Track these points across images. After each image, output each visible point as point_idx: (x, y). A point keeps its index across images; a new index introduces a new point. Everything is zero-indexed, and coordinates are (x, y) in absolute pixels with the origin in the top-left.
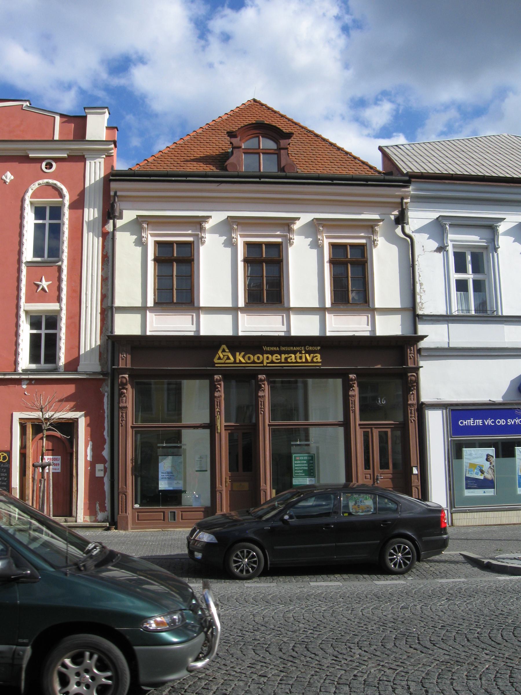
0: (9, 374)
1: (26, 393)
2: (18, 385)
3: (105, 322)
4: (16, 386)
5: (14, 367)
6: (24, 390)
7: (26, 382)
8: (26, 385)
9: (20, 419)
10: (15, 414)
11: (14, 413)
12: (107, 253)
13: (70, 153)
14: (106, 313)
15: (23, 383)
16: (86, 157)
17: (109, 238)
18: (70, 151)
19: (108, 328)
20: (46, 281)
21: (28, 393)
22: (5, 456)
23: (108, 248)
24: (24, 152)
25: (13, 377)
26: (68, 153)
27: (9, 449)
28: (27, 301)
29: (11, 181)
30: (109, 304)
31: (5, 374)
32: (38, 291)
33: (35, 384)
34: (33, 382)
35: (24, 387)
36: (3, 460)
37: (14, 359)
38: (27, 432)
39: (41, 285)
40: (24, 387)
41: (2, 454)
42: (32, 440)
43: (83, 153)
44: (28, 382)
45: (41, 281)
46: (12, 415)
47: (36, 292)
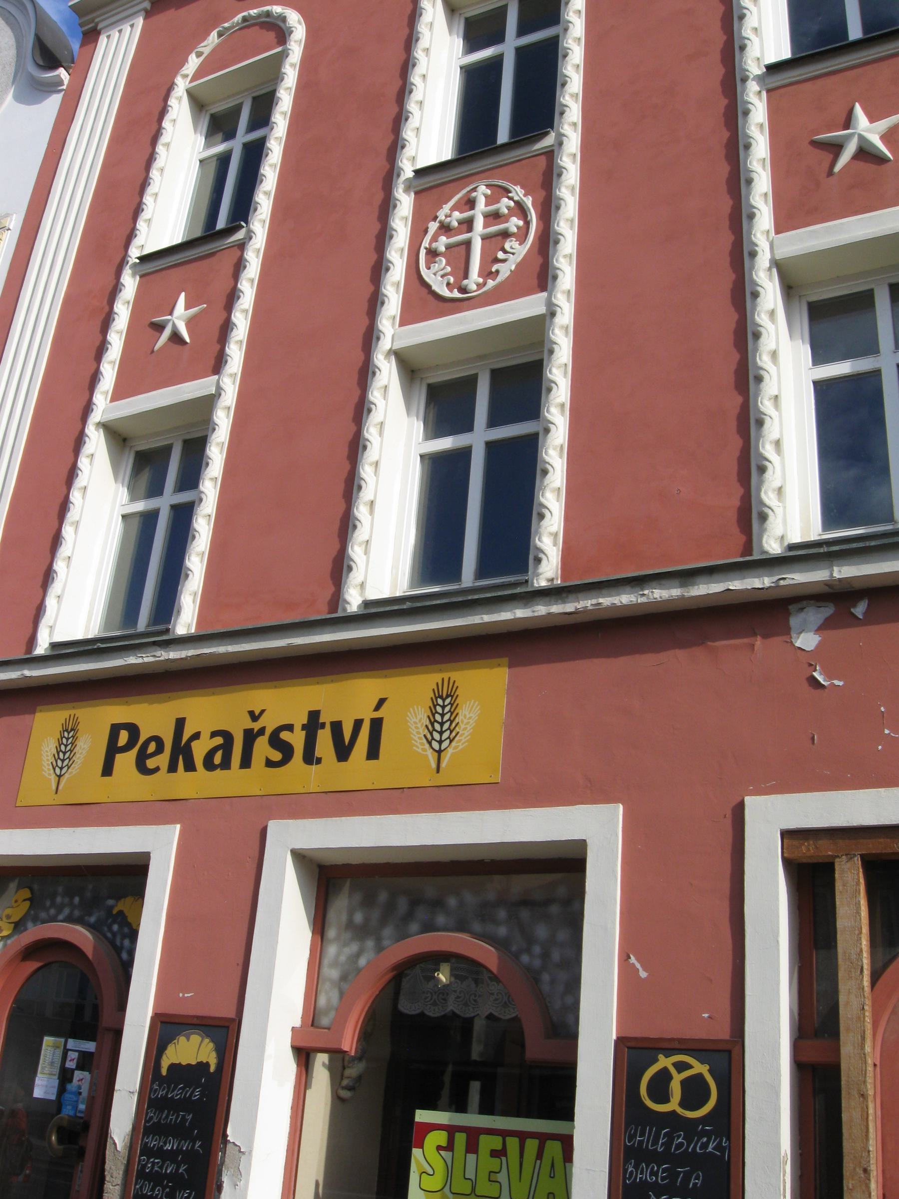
0: (710, 572)
1: (820, 678)
2: (765, 636)
4: (759, 642)
5: (743, 538)
6: (810, 659)
7: (815, 615)
8: (819, 629)
9: (786, 834)
10: (754, 805)
11: (750, 801)
15: (794, 621)
20: (873, 118)
21: (829, 676)
22: (699, 1077)
25: (738, 584)
27: (723, 1033)
31: (687, 576)
32: (837, 168)
33: (870, 619)
34: (860, 610)
35: (807, 641)
36: (683, 1104)
37: (736, 502)
38: (842, 923)
40: (807, 641)
41: (681, 1067)
42: (875, 977)
44: (828, 610)
45: (848, 122)
46: (739, 814)
47: (830, 173)
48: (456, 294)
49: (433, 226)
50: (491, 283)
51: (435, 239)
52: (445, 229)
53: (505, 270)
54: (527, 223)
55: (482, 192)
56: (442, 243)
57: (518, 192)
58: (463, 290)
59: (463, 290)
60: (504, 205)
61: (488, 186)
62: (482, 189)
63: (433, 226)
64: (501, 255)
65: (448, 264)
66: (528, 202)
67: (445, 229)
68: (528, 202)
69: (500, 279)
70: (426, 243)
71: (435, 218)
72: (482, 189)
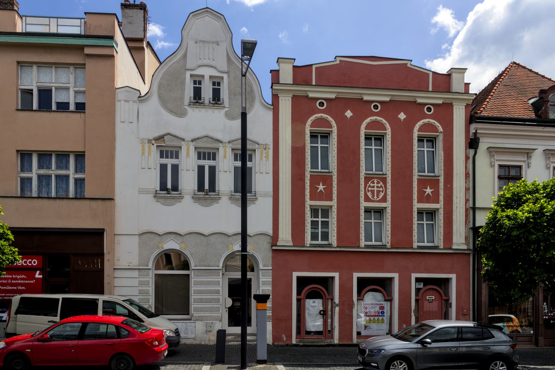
3: (468, 218)
12: (469, 172)
13: (444, 101)
14: (468, 211)
16: (453, 104)
17: (469, 161)
18: (444, 100)
19: (470, 221)
23: (469, 168)
24: (414, 98)
26: (443, 101)
28: (418, 202)
29: (404, 119)
30: (471, 205)
39: (427, 191)
43: (452, 101)
48: (373, 199)
49: (368, 185)
50: (378, 199)
51: (368, 188)
52: (370, 186)
53: (381, 197)
54: (383, 190)
55: (376, 181)
56: (370, 189)
57: (381, 183)
58: (374, 199)
59: (374, 199)
60: (379, 185)
61: (377, 180)
62: (376, 180)
63: (368, 185)
64: (380, 195)
65: (371, 193)
66: (383, 185)
67: (370, 186)
68: (383, 185)
69: (379, 199)
70: (367, 188)
71: (368, 184)
72: (376, 180)
